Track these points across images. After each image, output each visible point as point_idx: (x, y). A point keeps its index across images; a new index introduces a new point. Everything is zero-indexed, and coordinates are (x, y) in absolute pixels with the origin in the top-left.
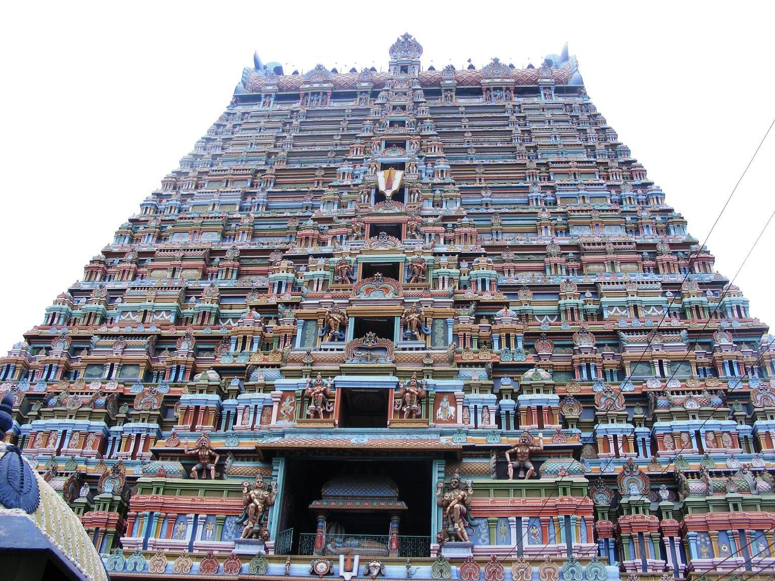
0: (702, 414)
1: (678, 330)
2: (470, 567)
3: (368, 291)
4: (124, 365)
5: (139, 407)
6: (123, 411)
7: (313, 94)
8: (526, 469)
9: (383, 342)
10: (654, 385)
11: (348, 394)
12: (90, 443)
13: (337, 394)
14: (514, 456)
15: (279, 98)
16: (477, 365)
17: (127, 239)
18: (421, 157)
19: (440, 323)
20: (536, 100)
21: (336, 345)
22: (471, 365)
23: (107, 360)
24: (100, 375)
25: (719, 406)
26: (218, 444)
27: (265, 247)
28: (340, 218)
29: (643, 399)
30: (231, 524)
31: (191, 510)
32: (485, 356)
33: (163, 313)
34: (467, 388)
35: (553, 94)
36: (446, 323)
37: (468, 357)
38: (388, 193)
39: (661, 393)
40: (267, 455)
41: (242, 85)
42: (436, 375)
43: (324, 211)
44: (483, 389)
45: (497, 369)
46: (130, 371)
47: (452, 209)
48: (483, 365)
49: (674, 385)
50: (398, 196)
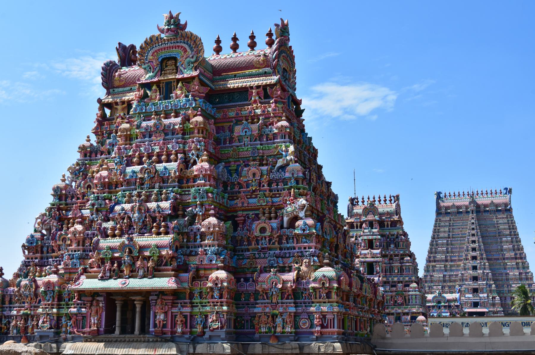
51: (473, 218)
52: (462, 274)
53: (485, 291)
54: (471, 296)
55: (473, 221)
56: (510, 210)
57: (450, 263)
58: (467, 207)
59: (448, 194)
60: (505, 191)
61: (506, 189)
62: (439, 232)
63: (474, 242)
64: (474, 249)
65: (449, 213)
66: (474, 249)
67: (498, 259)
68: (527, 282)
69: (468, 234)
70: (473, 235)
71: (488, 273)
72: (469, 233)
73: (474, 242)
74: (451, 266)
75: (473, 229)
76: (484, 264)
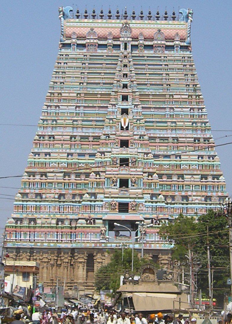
0: (199, 204)
2: (146, 245)
3: (122, 170)
4: (59, 183)
5: (66, 198)
6: (62, 199)
7: (91, 45)
8: (157, 222)
9: (126, 189)
10: (189, 193)
11: (120, 204)
12: (56, 209)
14: (155, 219)
16: (148, 194)
17: (42, 128)
18: (133, 104)
19: (139, 180)
20: (172, 52)
22: (146, 194)
23: (53, 182)
24: (52, 186)
25: (203, 201)
26: (93, 216)
27: (87, 134)
28: (111, 134)
29: (186, 198)
30: (98, 235)
31: (90, 232)
32: (150, 192)
33: (64, 163)
34: (146, 202)
35: (179, 50)
36: (141, 180)
37: (146, 192)
38: (125, 127)
39: (191, 196)
40: (104, 220)
42: (139, 198)
43: (107, 131)
44: (149, 202)
45: (152, 196)
46: (60, 185)
47: (142, 131)
48: (149, 194)
49: (194, 194)
50: (127, 128)
55: (125, 61)
58: (116, 38)
65: (84, 46)
68: (212, 173)
73: (125, 98)
75: (125, 75)
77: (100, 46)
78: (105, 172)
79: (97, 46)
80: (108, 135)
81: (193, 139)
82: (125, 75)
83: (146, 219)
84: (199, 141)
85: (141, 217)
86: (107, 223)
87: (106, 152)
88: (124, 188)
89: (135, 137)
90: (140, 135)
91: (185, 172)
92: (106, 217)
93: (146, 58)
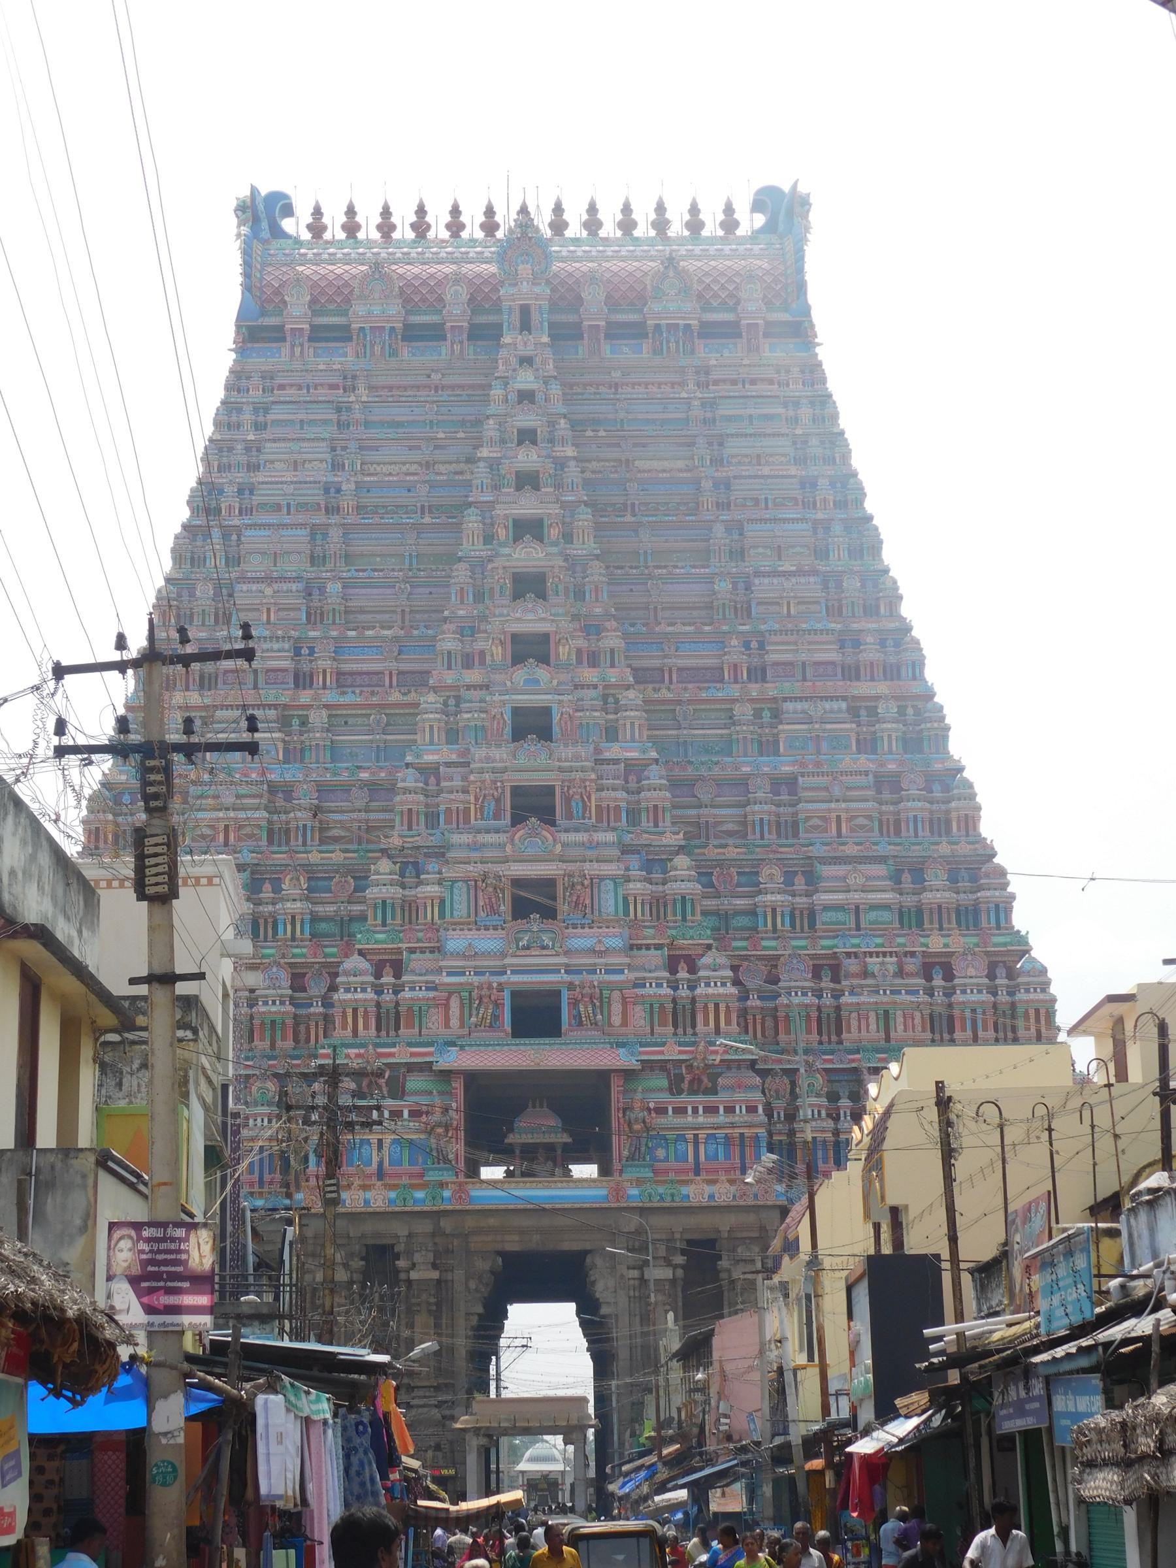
1: (882, 859)
13: (507, 995)
14: (690, 1067)
15: (318, 334)
21: (495, 920)
40: (446, 1075)
41: (247, 294)
48: (658, 947)
51: (526, 361)
52: (429, 772)
53: (609, 903)
54: (488, 942)
55: (526, 379)
56: (800, 330)
57: (330, 697)
59: (334, 221)
60: (760, 220)
61: (765, 200)
62: (253, 468)
63: (528, 529)
64: (529, 586)
65: (343, 334)
66: (529, 586)
67: (715, 675)
68: (944, 849)
69: (481, 472)
70: (527, 481)
71: (635, 770)
72: (494, 465)
73: (528, 529)
74: (337, 718)
75: (527, 437)
76: (609, 700)
77: (411, 334)
78: (440, 853)
79: (399, 332)
80: (457, 688)
81: (844, 705)
82: (527, 437)
83: (648, 1066)
84: (872, 712)
85: (624, 1059)
86: (458, 1085)
87: (448, 765)
88: (535, 923)
89: (581, 693)
90: (606, 687)
91: (818, 851)
92: (451, 1059)
93: (616, 375)
